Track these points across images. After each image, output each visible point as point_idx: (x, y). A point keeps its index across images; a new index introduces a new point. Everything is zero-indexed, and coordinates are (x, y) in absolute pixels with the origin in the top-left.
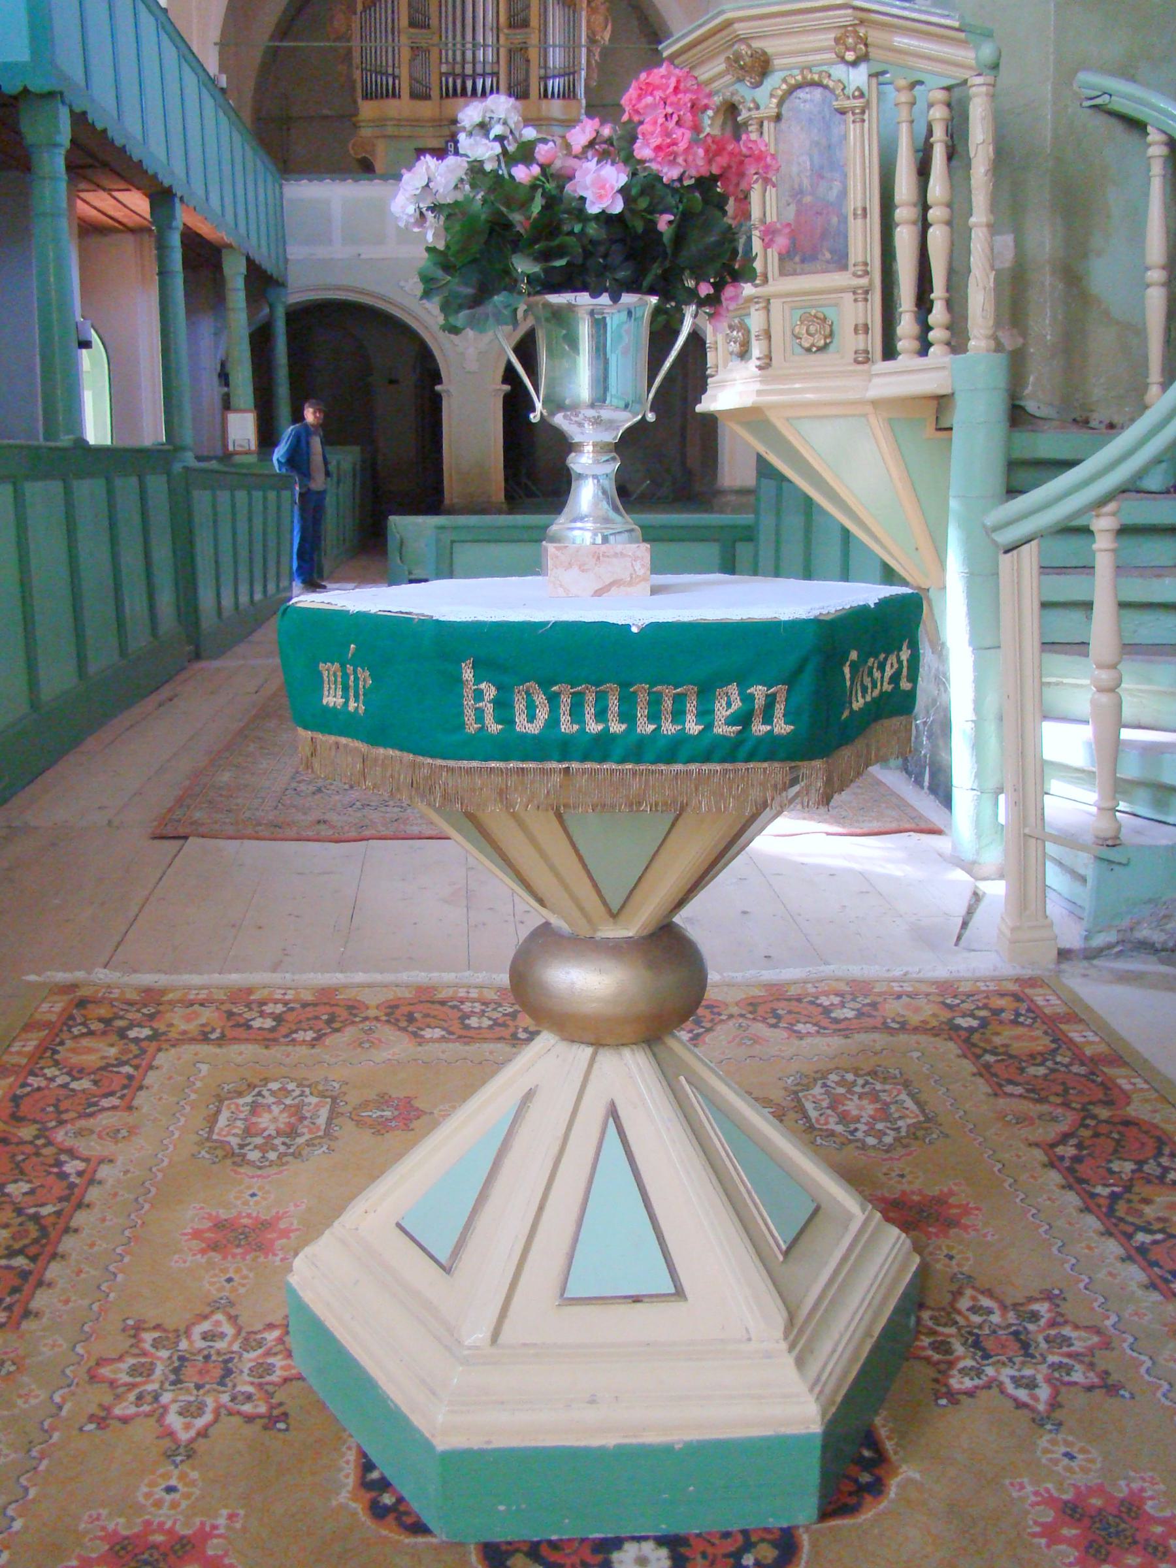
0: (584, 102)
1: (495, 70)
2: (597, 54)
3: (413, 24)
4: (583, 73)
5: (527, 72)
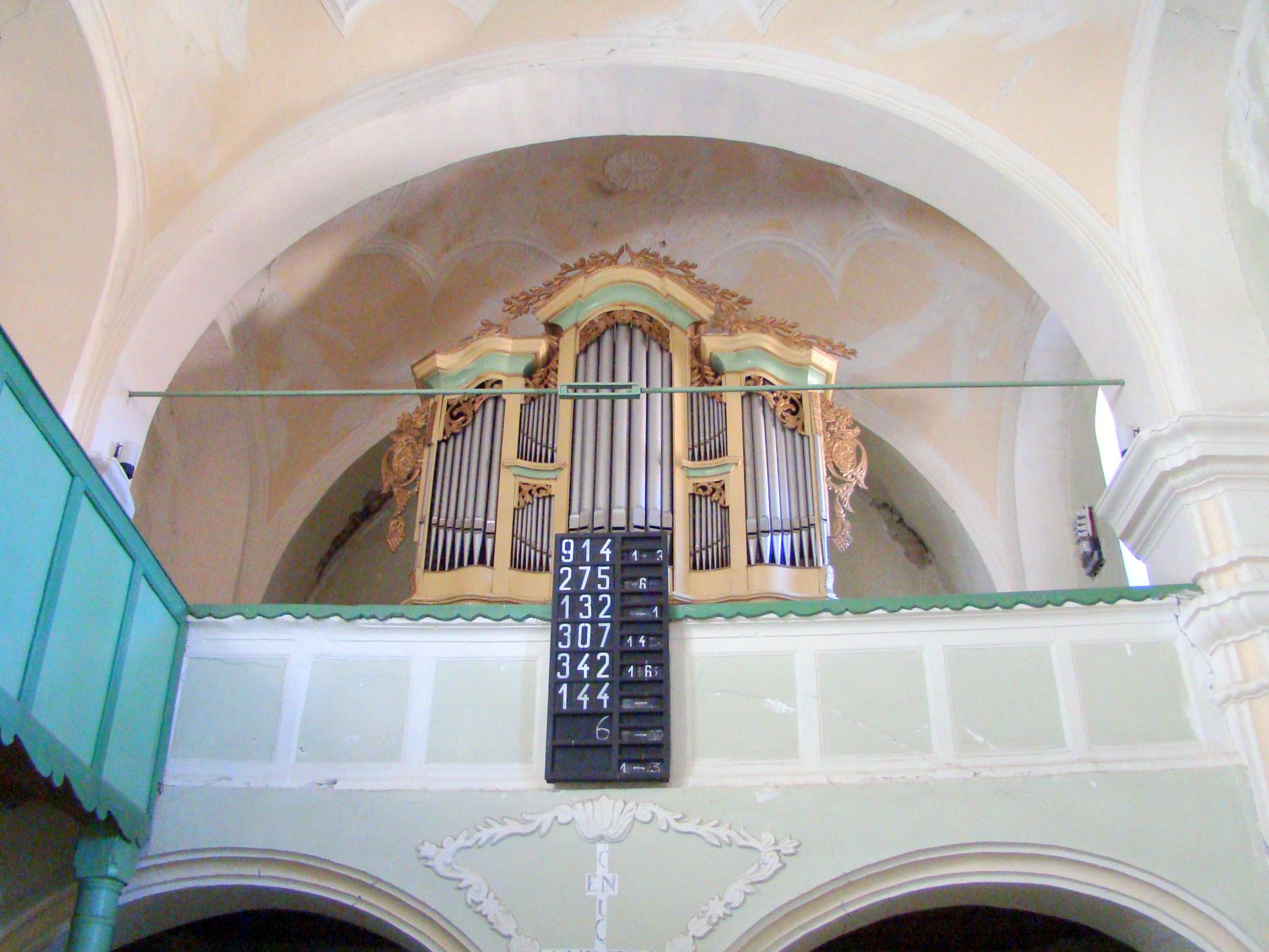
0: (830, 569)
1: (667, 524)
2: (847, 500)
3: (521, 455)
4: (826, 527)
5: (725, 525)
